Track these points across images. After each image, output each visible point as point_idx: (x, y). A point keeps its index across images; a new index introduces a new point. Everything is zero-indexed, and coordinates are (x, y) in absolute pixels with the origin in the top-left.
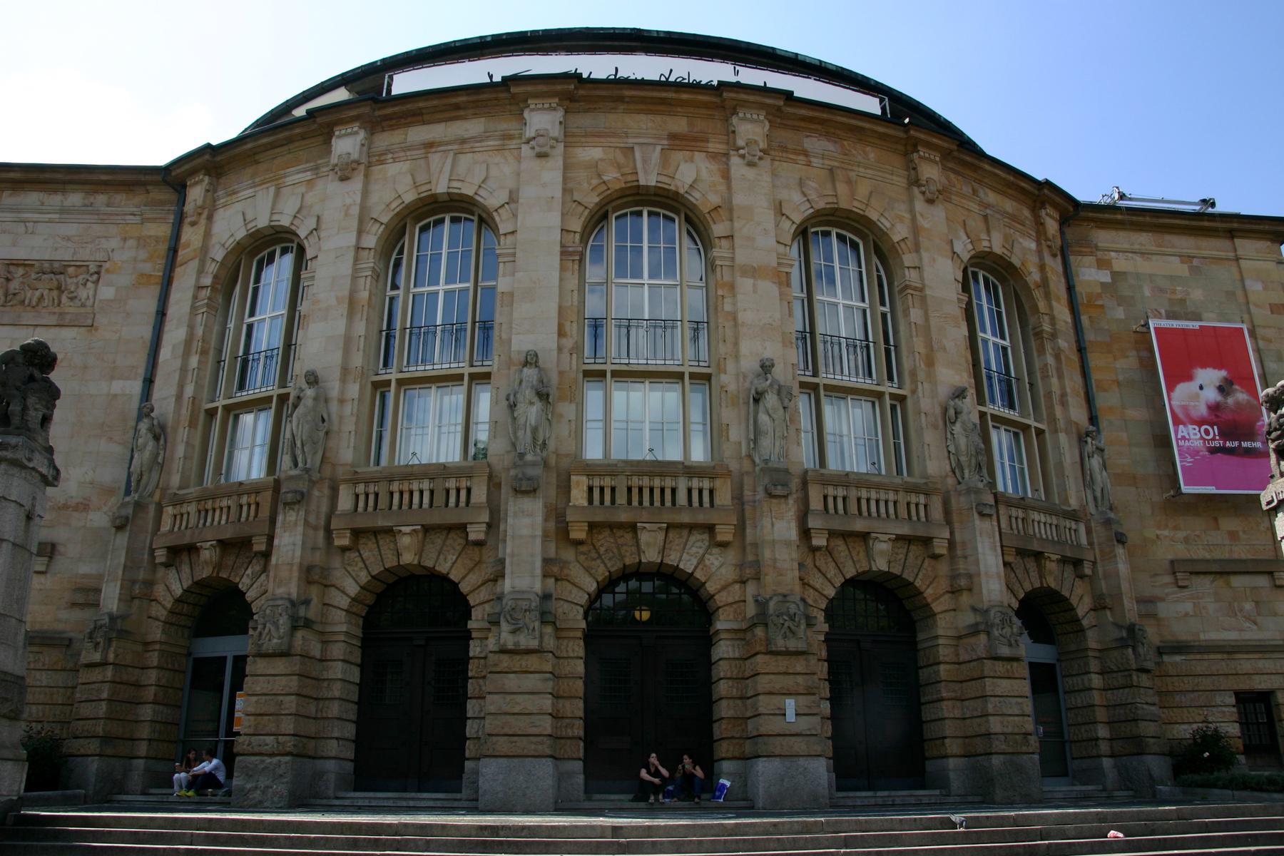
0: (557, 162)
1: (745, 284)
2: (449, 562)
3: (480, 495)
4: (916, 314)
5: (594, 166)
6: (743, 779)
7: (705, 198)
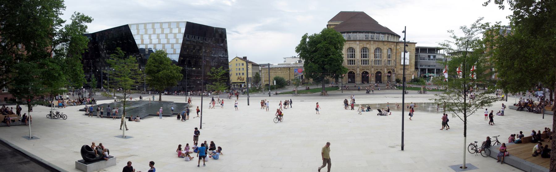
0: (359, 45)
1: (371, 54)
2: (353, 71)
3: (355, 67)
4: (383, 55)
5: (361, 46)
6: (370, 82)
7: (369, 48)
